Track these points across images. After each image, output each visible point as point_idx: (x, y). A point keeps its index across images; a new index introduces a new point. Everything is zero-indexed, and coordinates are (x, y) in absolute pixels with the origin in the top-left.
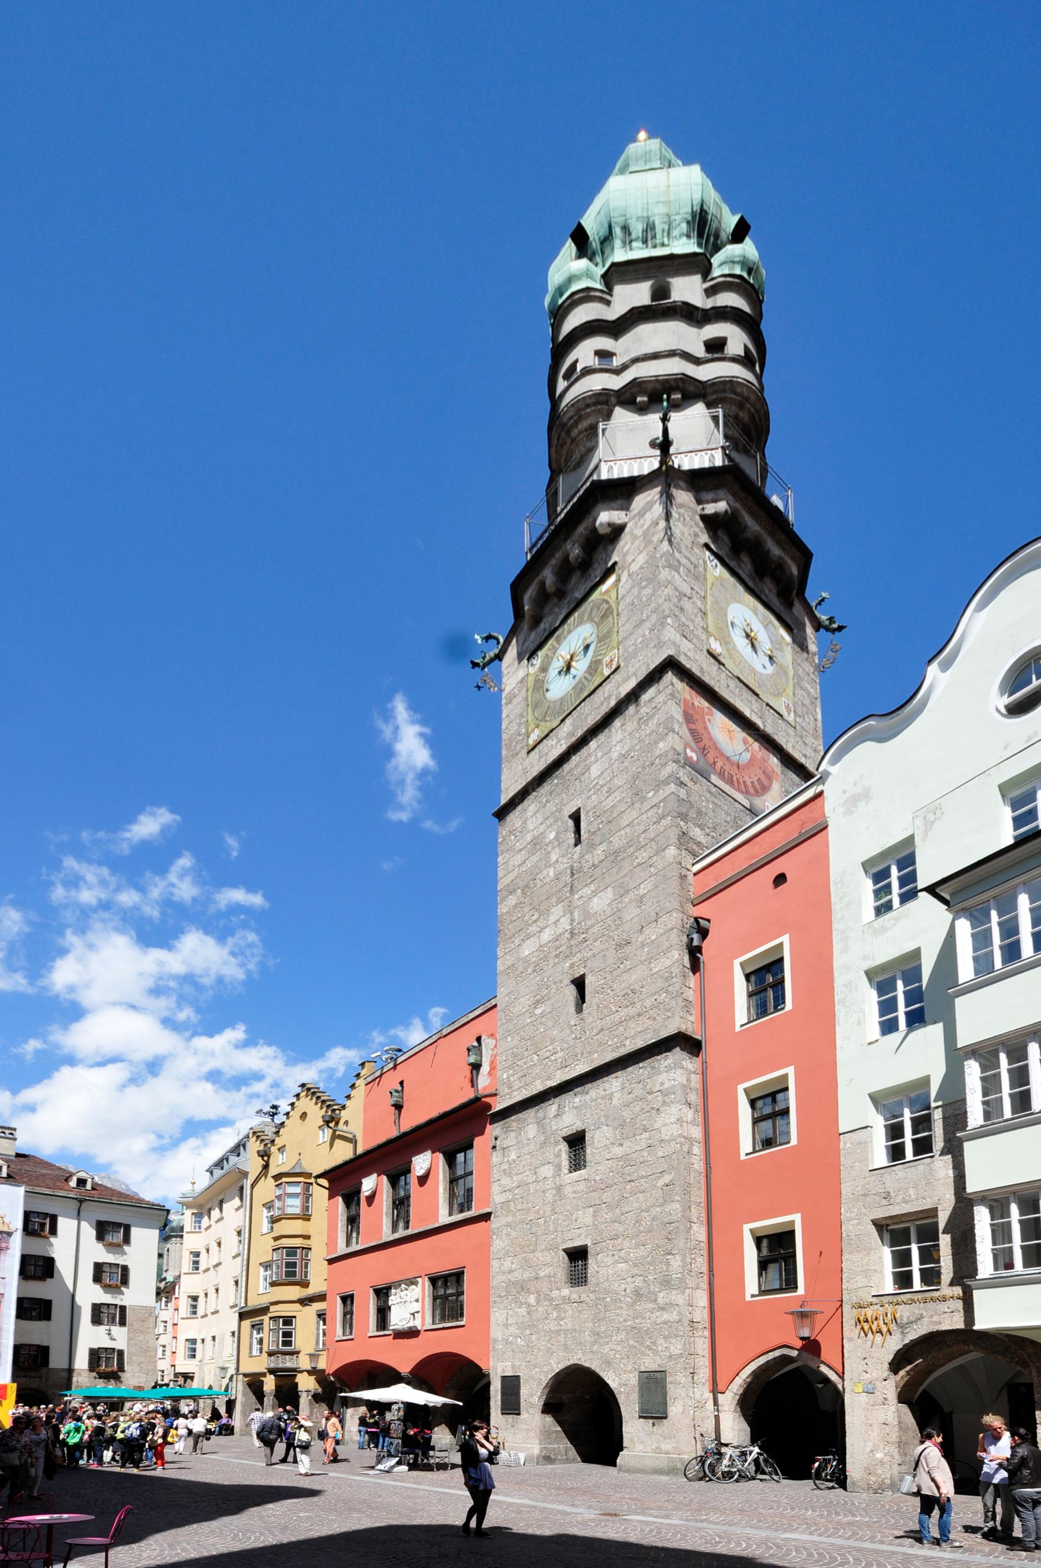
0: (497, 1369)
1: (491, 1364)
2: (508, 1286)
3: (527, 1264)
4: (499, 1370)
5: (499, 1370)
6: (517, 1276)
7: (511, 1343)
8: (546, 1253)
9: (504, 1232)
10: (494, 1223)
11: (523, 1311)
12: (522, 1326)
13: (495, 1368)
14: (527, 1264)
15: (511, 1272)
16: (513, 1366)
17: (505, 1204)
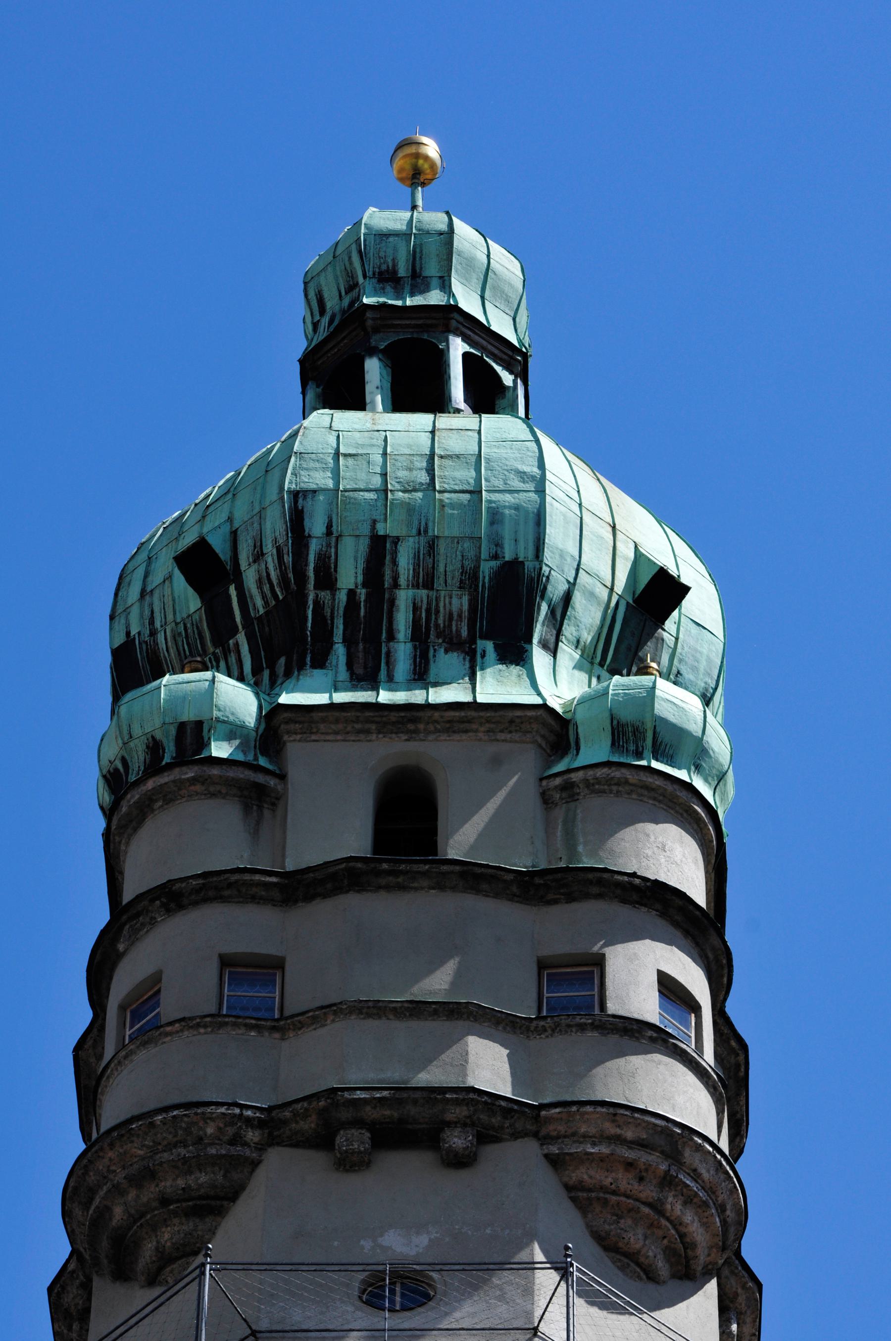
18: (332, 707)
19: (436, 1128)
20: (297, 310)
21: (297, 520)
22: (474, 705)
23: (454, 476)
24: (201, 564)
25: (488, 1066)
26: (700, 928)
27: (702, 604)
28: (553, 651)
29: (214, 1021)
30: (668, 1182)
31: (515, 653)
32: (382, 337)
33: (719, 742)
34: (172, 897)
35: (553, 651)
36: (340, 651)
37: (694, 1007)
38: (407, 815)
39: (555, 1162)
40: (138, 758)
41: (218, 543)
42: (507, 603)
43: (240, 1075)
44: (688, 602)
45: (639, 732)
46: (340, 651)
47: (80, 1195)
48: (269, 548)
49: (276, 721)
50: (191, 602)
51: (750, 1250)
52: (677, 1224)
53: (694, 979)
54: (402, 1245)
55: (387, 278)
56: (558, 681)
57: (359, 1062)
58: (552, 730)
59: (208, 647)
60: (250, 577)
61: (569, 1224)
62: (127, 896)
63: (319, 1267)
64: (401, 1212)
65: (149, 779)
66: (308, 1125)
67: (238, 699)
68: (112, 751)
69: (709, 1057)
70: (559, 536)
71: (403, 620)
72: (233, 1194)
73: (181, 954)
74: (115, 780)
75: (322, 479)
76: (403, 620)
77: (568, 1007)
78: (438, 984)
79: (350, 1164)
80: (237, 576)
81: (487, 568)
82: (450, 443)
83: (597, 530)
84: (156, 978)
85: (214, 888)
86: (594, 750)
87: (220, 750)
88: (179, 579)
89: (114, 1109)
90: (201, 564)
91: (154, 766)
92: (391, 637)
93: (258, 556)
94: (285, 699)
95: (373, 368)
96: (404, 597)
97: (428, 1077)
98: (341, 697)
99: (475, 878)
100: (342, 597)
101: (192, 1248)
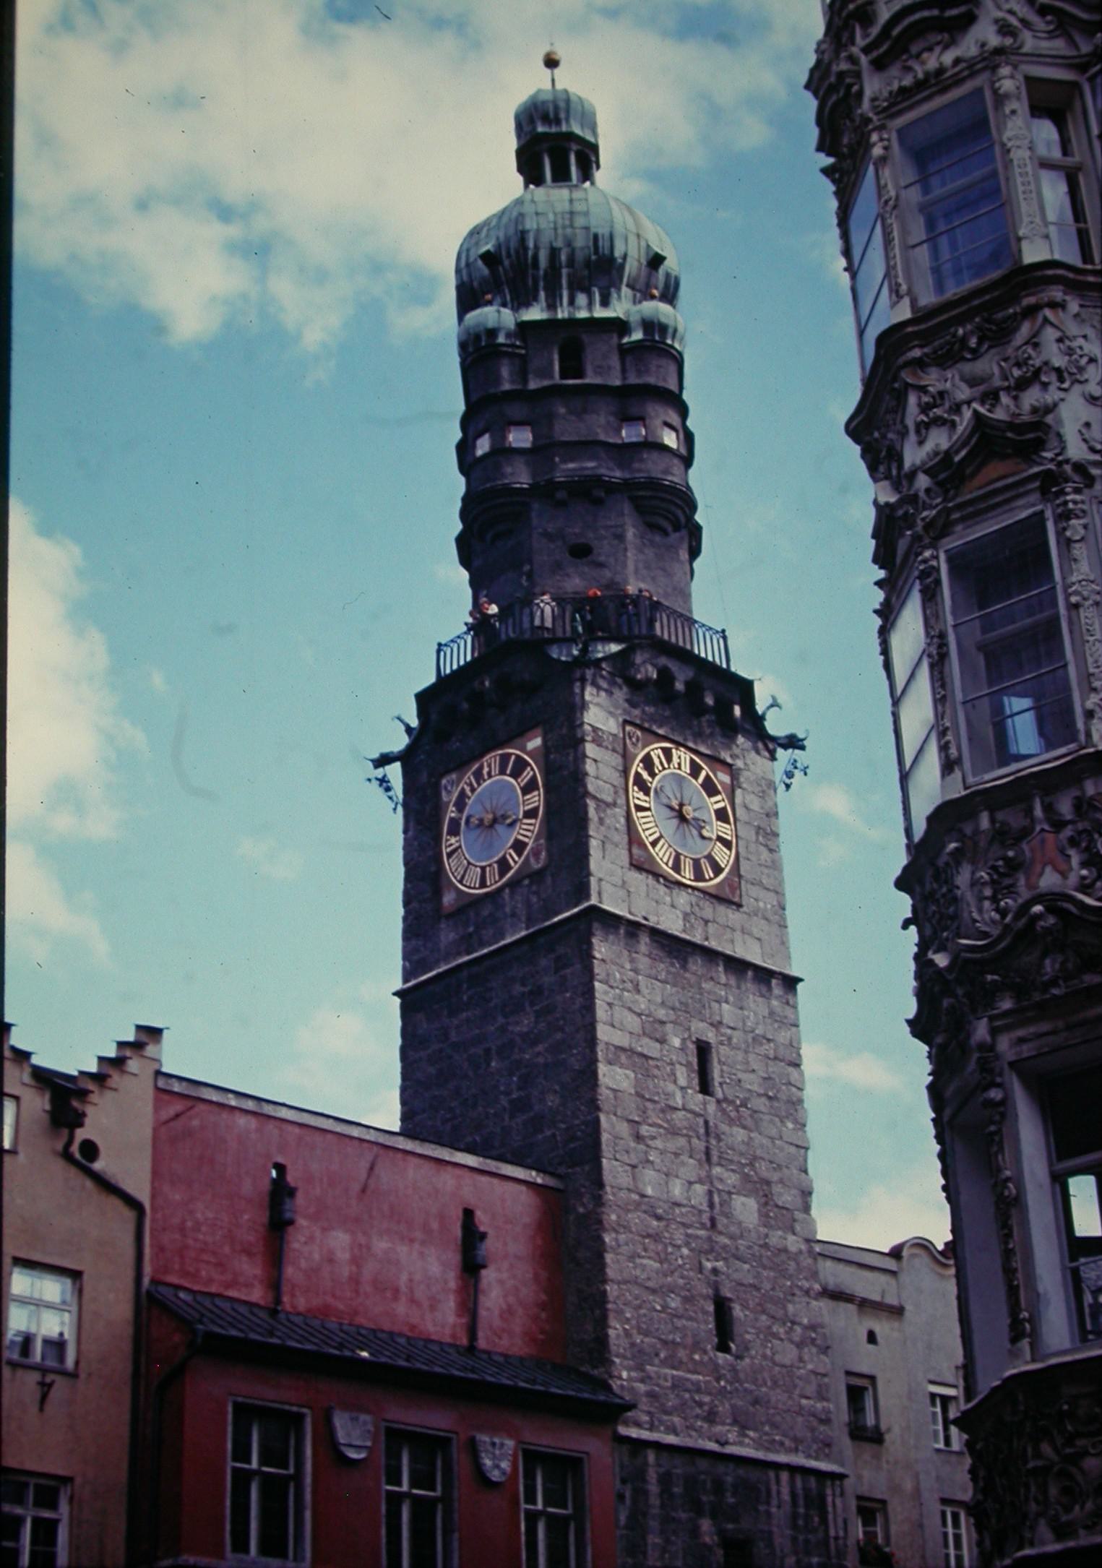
36: (542, 295)
44: (666, 263)
46: (542, 295)
48: (512, 252)
50: (486, 271)
52: (674, 515)
55: (546, 119)
60: (506, 263)
65: (478, 354)
71: (564, 282)
80: (501, 263)
82: (579, 207)
88: (480, 262)
90: (487, 258)
92: (561, 287)
96: (564, 271)
100: (541, 272)
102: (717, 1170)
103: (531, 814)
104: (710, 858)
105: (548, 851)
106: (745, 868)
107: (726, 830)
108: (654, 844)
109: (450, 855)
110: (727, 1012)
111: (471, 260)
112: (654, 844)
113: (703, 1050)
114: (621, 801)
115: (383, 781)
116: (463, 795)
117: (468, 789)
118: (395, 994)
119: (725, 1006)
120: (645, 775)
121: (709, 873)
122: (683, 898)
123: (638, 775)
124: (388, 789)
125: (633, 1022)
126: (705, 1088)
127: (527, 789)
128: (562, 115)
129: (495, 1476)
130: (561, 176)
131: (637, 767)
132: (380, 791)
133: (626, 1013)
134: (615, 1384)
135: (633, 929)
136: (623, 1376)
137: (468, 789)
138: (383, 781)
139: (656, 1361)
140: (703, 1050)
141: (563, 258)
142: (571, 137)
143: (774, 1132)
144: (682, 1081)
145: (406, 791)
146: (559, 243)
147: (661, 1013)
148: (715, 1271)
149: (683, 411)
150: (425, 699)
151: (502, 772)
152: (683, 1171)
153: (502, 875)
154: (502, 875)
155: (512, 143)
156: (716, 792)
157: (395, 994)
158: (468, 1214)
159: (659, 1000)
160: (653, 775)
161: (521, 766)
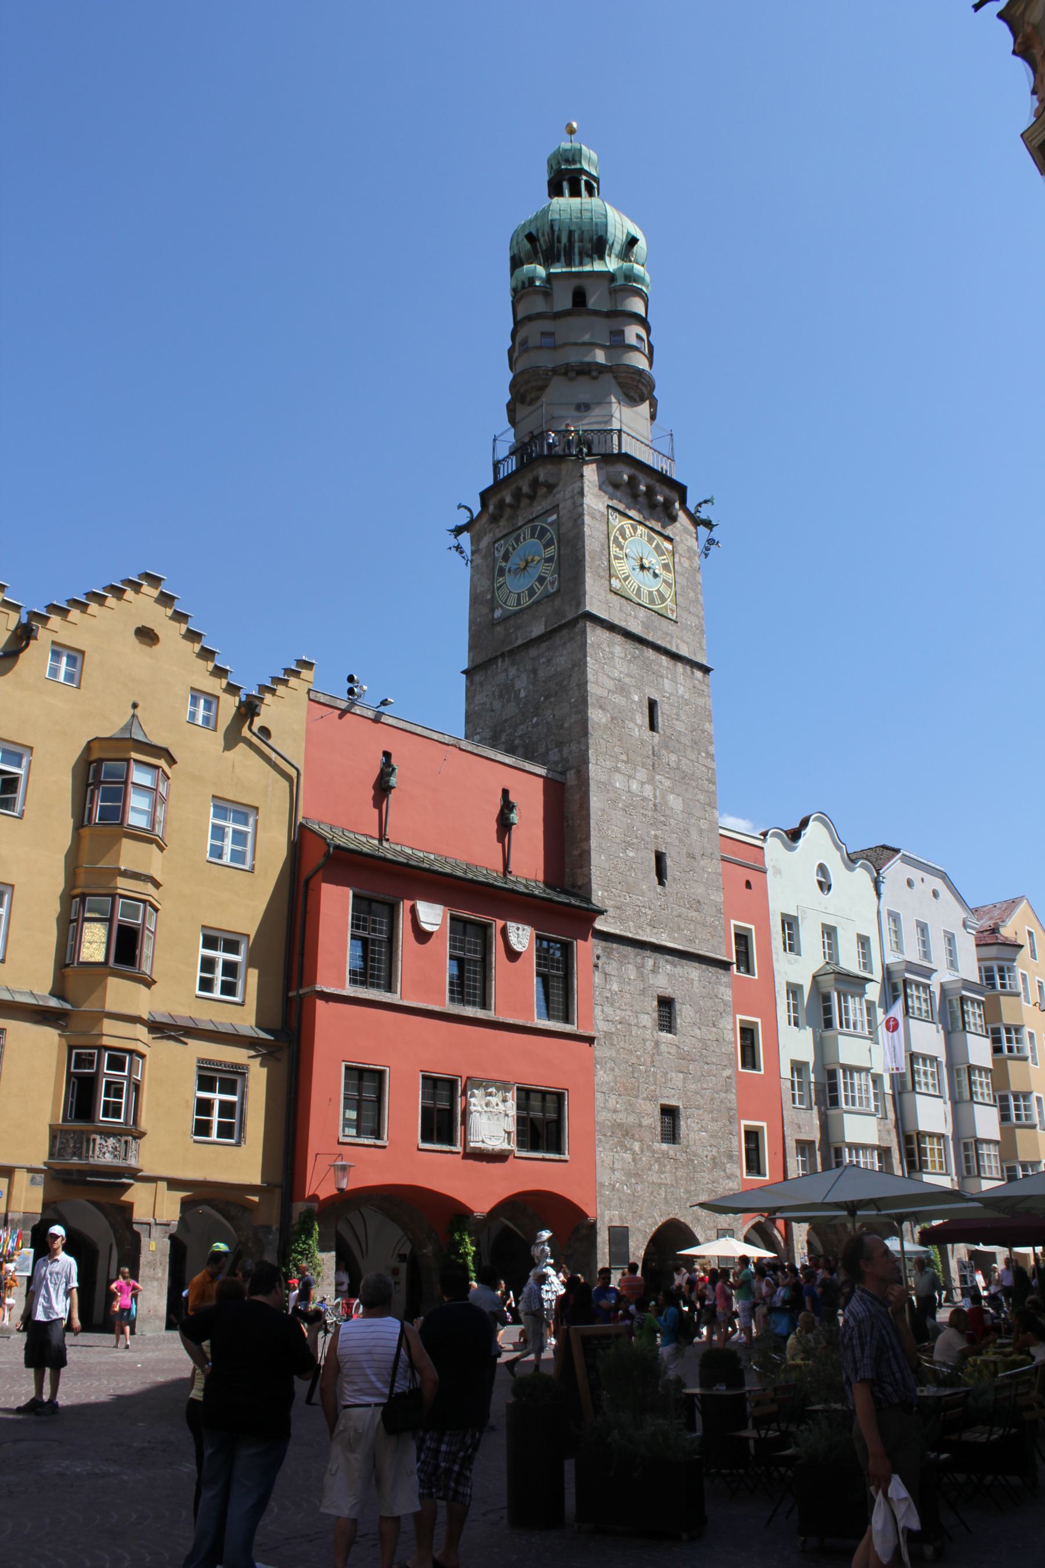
0: (606, 1217)
1: (599, 1211)
2: (613, 1126)
3: (630, 1108)
4: (607, 1218)
5: (607, 1218)
6: (621, 1117)
7: (618, 1190)
8: (647, 1102)
9: (608, 1065)
10: (600, 1050)
11: (628, 1156)
12: (629, 1175)
13: (603, 1216)
14: (630, 1108)
15: (615, 1111)
16: (621, 1218)
17: (608, 1034)
18: (562, 273)
19: (588, 371)
20: (545, 168)
21: (552, 227)
22: (593, 272)
23: (586, 215)
24: (531, 238)
25: (600, 357)
26: (643, 322)
27: (642, 244)
28: (610, 256)
29: (540, 348)
30: (639, 381)
31: (602, 258)
32: (566, 177)
33: (647, 278)
34: (529, 318)
35: (610, 256)
36: (563, 258)
37: (643, 340)
38: (580, 298)
39: (615, 378)
40: (520, 285)
41: (534, 232)
42: (599, 247)
43: (546, 360)
44: (639, 243)
45: (630, 276)
46: (563, 258)
47: (513, 386)
49: (550, 277)
50: (528, 246)
51: (655, 393)
53: (643, 334)
54: (584, 397)
55: (567, 161)
56: (611, 264)
57: (573, 357)
58: (611, 277)
59: (532, 258)
60: (542, 240)
61: (618, 390)
62: (519, 318)
63: (567, 404)
64: (582, 389)
65: (522, 291)
66: (563, 371)
67: (541, 271)
68: (514, 284)
69: (647, 351)
70: (610, 229)
71: (576, 251)
72: (546, 386)
73: (532, 331)
74: (515, 291)
75: (557, 217)
76: (576, 251)
77: (618, 344)
78: (586, 338)
79: (571, 379)
80: (538, 240)
81: (595, 237)
82: (585, 206)
83: (619, 226)
84: (527, 337)
85: (540, 316)
86: (620, 281)
87: (538, 283)
88: (525, 241)
89: (519, 367)
90: (531, 238)
91: (523, 287)
93: (543, 235)
94: (552, 271)
95: (565, 185)
96: (577, 245)
97: (587, 359)
98: (564, 270)
99: (596, 313)
101: (538, 398)
102: (658, 777)
103: (549, 560)
104: (658, 591)
105: (559, 581)
106: (680, 600)
107: (670, 577)
108: (626, 579)
109: (499, 588)
110: (667, 684)
111: (520, 240)
112: (626, 579)
113: (652, 705)
114: (606, 552)
115: (458, 548)
116: (507, 553)
117: (510, 549)
118: (463, 672)
119: (666, 681)
120: (621, 539)
121: (658, 601)
122: (642, 613)
123: (616, 538)
124: (462, 552)
125: (610, 684)
126: (653, 727)
127: (546, 546)
128: (577, 158)
129: (518, 948)
130: (575, 193)
131: (614, 533)
132: (457, 553)
133: (605, 677)
134: (594, 901)
135: (611, 627)
136: (598, 896)
137: (510, 549)
138: (458, 548)
139: (619, 887)
140: (652, 705)
141: (576, 236)
142: (582, 171)
143: (694, 757)
144: (639, 722)
145: (473, 553)
146: (572, 228)
147: (627, 680)
148: (656, 836)
149: (648, 331)
150: (485, 496)
151: (532, 537)
152: (639, 776)
153: (530, 597)
154: (530, 597)
155: (546, 178)
156: (663, 554)
157: (463, 672)
158: (505, 793)
159: (626, 671)
160: (625, 538)
161: (544, 531)
